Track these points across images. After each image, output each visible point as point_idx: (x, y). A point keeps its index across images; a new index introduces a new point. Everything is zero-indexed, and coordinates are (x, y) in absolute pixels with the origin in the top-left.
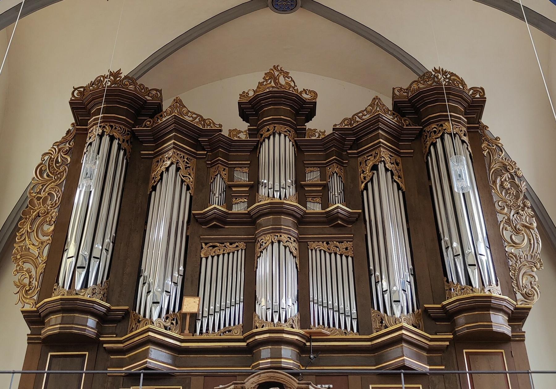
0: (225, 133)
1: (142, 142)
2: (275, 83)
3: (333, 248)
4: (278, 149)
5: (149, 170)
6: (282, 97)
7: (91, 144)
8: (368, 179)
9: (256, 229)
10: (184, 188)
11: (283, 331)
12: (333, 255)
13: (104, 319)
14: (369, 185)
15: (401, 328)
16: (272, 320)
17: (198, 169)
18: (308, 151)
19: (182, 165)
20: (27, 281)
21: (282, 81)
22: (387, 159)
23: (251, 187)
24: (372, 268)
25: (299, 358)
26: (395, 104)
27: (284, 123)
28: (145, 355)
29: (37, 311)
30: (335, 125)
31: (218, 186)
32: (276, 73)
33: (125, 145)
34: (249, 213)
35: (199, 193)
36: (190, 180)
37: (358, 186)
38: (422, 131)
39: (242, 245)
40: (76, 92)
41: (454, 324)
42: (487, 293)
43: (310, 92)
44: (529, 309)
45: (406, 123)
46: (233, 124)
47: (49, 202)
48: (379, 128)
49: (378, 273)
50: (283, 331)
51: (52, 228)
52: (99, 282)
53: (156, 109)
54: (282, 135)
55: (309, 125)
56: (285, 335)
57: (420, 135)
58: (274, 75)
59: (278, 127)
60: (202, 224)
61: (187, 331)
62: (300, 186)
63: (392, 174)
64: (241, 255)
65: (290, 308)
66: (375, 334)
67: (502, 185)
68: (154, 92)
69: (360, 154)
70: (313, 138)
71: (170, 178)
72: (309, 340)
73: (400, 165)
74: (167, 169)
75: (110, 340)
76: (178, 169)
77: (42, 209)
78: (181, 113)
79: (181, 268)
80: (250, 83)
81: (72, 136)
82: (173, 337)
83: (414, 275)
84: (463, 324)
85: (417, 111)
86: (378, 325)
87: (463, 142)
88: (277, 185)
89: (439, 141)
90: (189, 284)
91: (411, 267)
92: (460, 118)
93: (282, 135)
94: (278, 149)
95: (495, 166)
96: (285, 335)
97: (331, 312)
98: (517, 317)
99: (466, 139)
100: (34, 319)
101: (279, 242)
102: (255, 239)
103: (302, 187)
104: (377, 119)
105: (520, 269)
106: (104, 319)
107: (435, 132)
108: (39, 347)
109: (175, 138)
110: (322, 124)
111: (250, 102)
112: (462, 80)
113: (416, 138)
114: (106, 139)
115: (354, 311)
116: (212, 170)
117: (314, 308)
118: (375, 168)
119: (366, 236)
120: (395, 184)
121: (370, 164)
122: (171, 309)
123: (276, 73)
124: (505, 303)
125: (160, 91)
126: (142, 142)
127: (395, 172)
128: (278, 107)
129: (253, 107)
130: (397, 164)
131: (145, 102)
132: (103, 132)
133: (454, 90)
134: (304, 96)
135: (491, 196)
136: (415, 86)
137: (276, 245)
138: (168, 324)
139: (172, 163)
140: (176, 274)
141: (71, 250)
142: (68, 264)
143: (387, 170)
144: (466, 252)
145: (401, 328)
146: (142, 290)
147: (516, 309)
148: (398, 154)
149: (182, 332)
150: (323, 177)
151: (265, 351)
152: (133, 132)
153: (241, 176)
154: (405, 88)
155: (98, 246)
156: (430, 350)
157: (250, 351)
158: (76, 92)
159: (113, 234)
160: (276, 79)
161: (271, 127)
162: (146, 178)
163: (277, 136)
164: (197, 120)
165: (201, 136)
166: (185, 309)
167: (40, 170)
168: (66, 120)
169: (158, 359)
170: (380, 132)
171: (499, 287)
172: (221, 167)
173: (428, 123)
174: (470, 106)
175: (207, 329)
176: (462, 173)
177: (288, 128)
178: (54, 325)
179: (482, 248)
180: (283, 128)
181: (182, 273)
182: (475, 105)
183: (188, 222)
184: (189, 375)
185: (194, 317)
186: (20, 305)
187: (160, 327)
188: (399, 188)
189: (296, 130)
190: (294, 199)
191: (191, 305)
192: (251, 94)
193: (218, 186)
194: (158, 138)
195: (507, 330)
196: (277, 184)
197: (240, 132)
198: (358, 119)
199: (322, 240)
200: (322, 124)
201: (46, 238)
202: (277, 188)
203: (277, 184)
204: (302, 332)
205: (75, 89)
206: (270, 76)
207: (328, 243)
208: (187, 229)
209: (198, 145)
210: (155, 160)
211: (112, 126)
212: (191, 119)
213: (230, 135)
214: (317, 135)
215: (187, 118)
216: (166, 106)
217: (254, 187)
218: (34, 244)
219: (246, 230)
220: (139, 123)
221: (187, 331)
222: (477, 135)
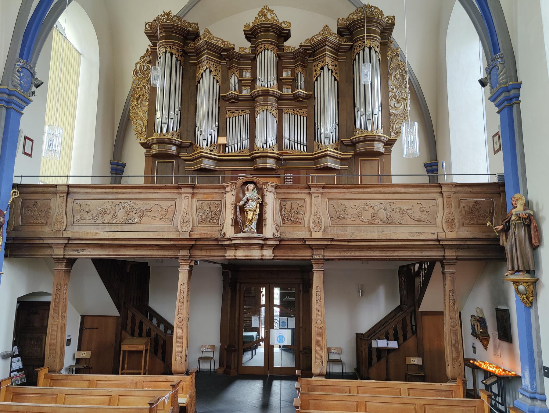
0: (237, 50)
1: (190, 56)
2: (265, 18)
3: (296, 113)
4: (267, 58)
5: (195, 72)
6: (269, 27)
7: (160, 57)
8: (318, 75)
9: (255, 103)
10: (215, 81)
11: (267, 152)
12: (296, 116)
13: (180, 146)
14: (319, 78)
15: (327, 151)
16: (263, 147)
17: (222, 71)
19: (213, 69)
20: (140, 129)
21: (269, 16)
22: (330, 63)
23: (252, 80)
24: (316, 122)
25: (277, 163)
26: (338, 29)
27: (270, 43)
28: (201, 162)
29: (146, 143)
30: (301, 43)
31: (234, 80)
32: (266, 11)
33: (179, 58)
34: (251, 95)
36: (218, 77)
37: (312, 79)
38: (352, 46)
39: (248, 111)
40: (147, 25)
41: (355, 147)
42: (375, 134)
43: (287, 22)
44: (396, 140)
45: (344, 42)
46: (241, 44)
47: (144, 90)
48: (326, 45)
49: (319, 124)
50: (267, 152)
51: (147, 103)
52: (175, 130)
53: (197, 36)
54: (269, 51)
55: (286, 44)
56: (268, 154)
57: (351, 48)
58: (264, 12)
59: (267, 46)
60: (226, 101)
61: (221, 152)
62: (279, 80)
63: (332, 72)
64: (247, 116)
65: (273, 141)
66: (315, 153)
67: (395, 76)
68: (193, 25)
69: (314, 60)
70: (288, 51)
71: (206, 75)
72: (281, 155)
73: (338, 66)
74: (205, 71)
75: (184, 156)
76: (211, 71)
77: (141, 94)
78: (209, 39)
79: (217, 123)
80: (250, 17)
81: (150, 53)
82: (215, 154)
83: (338, 125)
84: (361, 147)
85: (351, 33)
86: (317, 148)
87: (376, 52)
89: (361, 52)
90: (222, 130)
91: (337, 121)
92: (376, 37)
93: (269, 51)
94: (267, 58)
95: (393, 65)
96: (268, 154)
97: (293, 143)
98: (389, 144)
99: (378, 50)
100: (147, 146)
101: (267, 110)
102: (255, 108)
103: (281, 80)
104: (325, 40)
105: (395, 121)
106: (180, 146)
107: (360, 46)
108: (151, 158)
109: (208, 53)
110: (293, 43)
111: (250, 30)
112: (381, 12)
113: (349, 50)
114: (168, 55)
115: (305, 142)
116: (230, 71)
117: (285, 141)
118: (322, 68)
119: (315, 106)
120: (333, 78)
121: (320, 66)
122: (213, 141)
123: (266, 11)
124: (383, 138)
125: (197, 24)
126: (190, 56)
127: (334, 71)
128: (268, 33)
129: (252, 34)
130: (336, 66)
131: (189, 31)
132: (166, 51)
133: (375, 19)
134: (283, 25)
135: (388, 83)
136: (351, 17)
137: (265, 112)
138: (212, 149)
139: (207, 68)
140: (214, 126)
141: (159, 114)
142: (158, 122)
143: (329, 70)
144: (367, 113)
145: (327, 151)
146: (198, 133)
147: (389, 140)
148: (336, 59)
149: (219, 152)
150: (293, 74)
151: (259, 160)
152: (183, 50)
153: (247, 75)
154: (346, 18)
155: (172, 113)
156: (342, 159)
157: (253, 160)
158: (147, 25)
159: (180, 106)
160: (265, 15)
161: (263, 46)
162: (194, 77)
163: (266, 51)
164: (220, 42)
165: (222, 52)
166: (219, 142)
167: (136, 73)
168: (145, 43)
169: (207, 164)
170: (327, 47)
171: (382, 130)
172: (235, 70)
173: (356, 41)
174: (384, 29)
175: (232, 151)
177: (273, 46)
178: (155, 149)
179: (377, 111)
180: (270, 46)
181: (217, 125)
182: (388, 28)
183: (219, 100)
184: (224, 170)
185: (225, 145)
186: (139, 140)
187: (207, 150)
188: (335, 79)
189: (278, 47)
190: (275, 87)
191: (222, 140)
192: (251, 25)
193: (234, 80)
194: (198, 53)
195: (382, 150)
196: (266, 79)
197: (245, 49)
198: (315, 39)
199: (291, 108)
200: (293, 43)
201: (145, 108)
202: (266, 81)
203: (266, 79)
204: (277, 152)
205: (147, 24)
206: (262, 13)
207: (293, 110)
208: (219, 103)
209: (221, 57)
210: (198, 66)
211: (170, 47)
212: (216, 42)
213: (239, 51)
214: (290, 49)
215: (214, 42)
216: (202, 32)
217: (254, 80)
220: (186, 44)
221: (221, 152)
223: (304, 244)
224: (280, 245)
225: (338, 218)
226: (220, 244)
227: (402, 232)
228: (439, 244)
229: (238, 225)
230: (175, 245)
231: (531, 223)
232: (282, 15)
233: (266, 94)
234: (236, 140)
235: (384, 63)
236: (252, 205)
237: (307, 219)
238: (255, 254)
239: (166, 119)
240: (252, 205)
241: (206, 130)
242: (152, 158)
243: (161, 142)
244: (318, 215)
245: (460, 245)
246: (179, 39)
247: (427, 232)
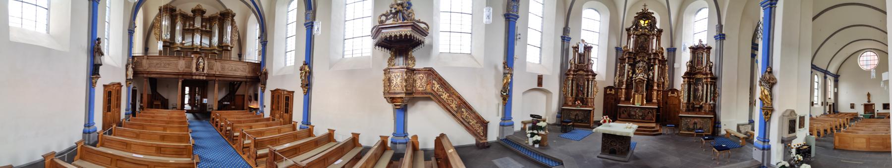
18: (203, 20)
35: (184, 25)
46: (190, 14)
80: (193, 5)
88: (198, 25)
90: (183, 39)
110: (207, 15)
128: (198, 12)
176: (229, 29)
182: (233, 16)
194: (176, 16)
200: (207, 15)
219: (192, 32)
222: (233, 20)
223: (214, 75)
224: (208, 75)
225: (223, 69)
226: (191, 74)
227: (238, 74)
228: (246, 77)
229: (197, 69)
230: (178, 74)
231: (266, 74)
232: (204, 7)
233: (198, 29)
235: (232, 25)
236: (202, 64)
237: (215, 68)
238: (201, 78)
239: (166, 36)
240: (202, 64)
245: (251, 78)
246: (170, 11)
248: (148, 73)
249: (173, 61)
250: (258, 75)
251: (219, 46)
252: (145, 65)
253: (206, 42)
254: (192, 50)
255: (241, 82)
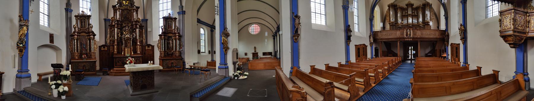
18: (413, 9)
35: (402, 13)
46: (405, 7)
80: (407, 2)
90: (402, 21)
110: (414, 6)
128: (410, 5)
194: (397, 8)
200: (414, 6)
218: (388, 18)
219: (407, 16)
224: (413, 38)
225: (422, 34)
226: (404, 38)
227: (432, 37)
228: (437, 38)
229: (407, 35)
231: (448, 36)
232: (412, 2)
234: (405, 22)
237: (417, 34)
239: (392, 20)
241: (400, 21)
242: (390, 26)
243: (392, 23)
244: (419, 34)
245: (440, 39)
247: (435, 37)
248: (381, 39)
249: (394, 32)
250: (445, 35)
251: (423, 23)
252: (380, 36)
253: (415, 21)
254: (408, 26)
255: (436, 41)
